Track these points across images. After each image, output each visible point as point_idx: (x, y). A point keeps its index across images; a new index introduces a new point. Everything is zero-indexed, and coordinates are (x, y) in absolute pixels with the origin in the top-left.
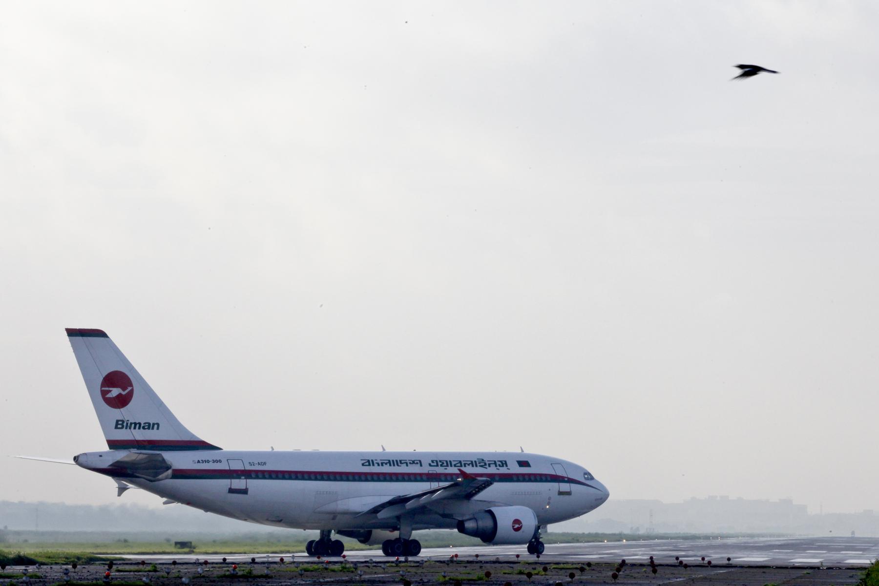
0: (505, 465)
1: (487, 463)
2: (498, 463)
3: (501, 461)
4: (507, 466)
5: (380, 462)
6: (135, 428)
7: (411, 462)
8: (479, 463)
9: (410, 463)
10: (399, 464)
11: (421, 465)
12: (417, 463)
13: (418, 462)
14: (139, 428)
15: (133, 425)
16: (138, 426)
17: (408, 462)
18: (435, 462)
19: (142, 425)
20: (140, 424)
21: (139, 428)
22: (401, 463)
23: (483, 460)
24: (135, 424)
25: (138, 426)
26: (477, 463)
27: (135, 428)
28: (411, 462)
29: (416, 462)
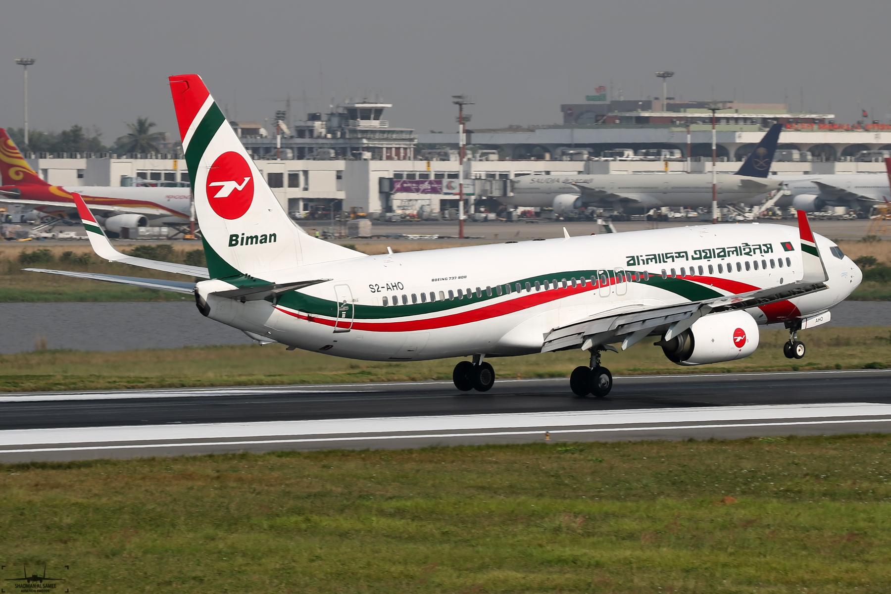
0: (770, 250)
1: (752, 248)
2: (763, 248)
4: (772, 252)
5: (645, 258)
7: (677, 255)
9: (676, 257)
10: (666, 260)
11: (687, 259)
12: (683, 256)
15: (250, 240)
16: (254, 239)
17: (674, 255)
18: (698, 252)
19: (259, 239)
20: (256, 237)
22: (667, 258)
24: (252, 238)
25: (254, 239)
26: (742, 248)
27: (252, 243)
29: (681, 254)
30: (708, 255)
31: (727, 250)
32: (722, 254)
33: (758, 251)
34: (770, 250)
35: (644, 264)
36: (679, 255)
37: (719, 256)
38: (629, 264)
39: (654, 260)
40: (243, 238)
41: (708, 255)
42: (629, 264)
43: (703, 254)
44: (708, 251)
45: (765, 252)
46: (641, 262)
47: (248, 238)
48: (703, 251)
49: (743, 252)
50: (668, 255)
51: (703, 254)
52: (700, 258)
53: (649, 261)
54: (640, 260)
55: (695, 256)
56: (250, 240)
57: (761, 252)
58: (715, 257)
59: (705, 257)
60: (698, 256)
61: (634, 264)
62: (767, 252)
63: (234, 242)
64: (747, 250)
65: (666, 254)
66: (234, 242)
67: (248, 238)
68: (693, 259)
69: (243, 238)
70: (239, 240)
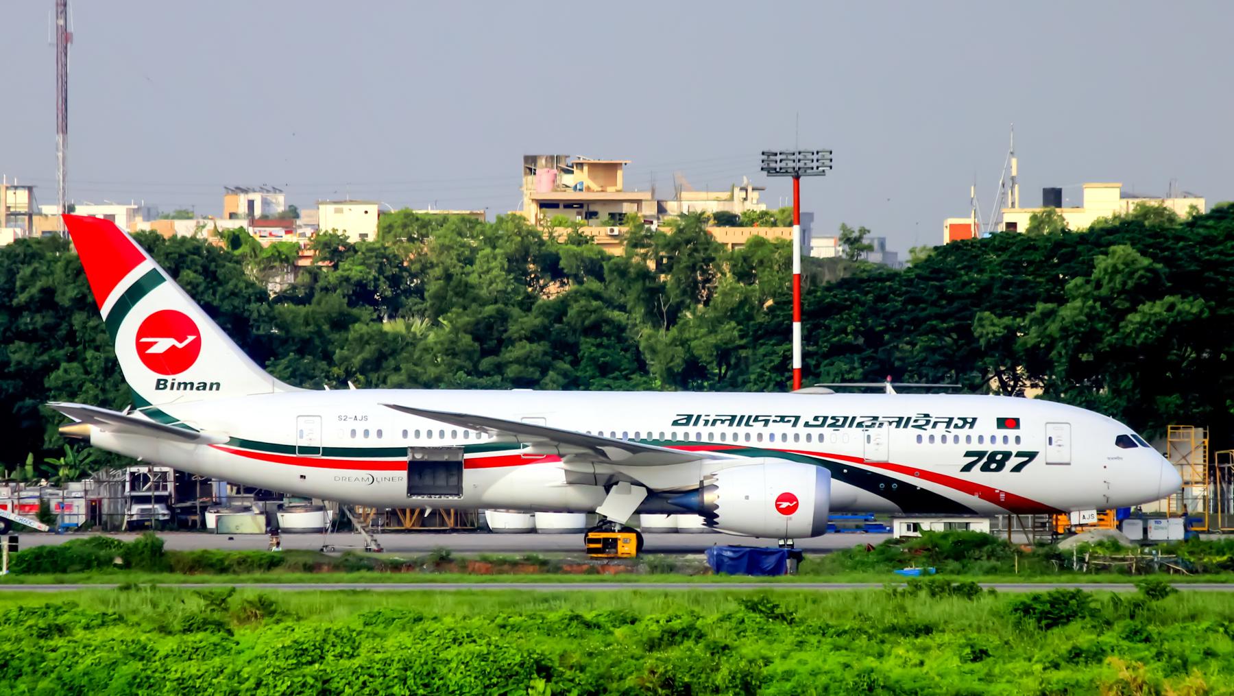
0: (968, 425)
1: (933, 420)
2: (955, 421)
3: (964, 420)
4: (971, 427)
5: (711, 419)
6: (185, 388)
8: (916, 421)
9: (774, 421)
10: (751, 423)
11: (795, 425)
12: (789, 421)
13: (793, 419)
14: (192, 389)
15: (182, 386)
16: (189, 386)
18: (821, 419)
20: (192, 384)
21: (192, 389)
22: (756, 419)
23: (927, 416)
24: (185, 384)
25: (189, 386)
27: (185, 388)
28: (778, 419)
29: (786, 419)
30: (840, 423)
31: (881, 419)
32: (869, 423)
33: (941, 427)
34: (968, 425)
35: (707, 422)
36: (782, 419)
37: (860, 425)
38: (675, 423)
39: (728, 422)
40: (173, 384)
41: (840, 423)
42: (675, 423)
43: (830, 421)
44: (842, 420)
45: (956, 426)
46: (701, 422)
47: (179, 384)
48: (833, 418)
49: (912, 423)
50: (760, 418)
51: (830, 421)
52: (822, 425)
53: (719, 422)
54: (703, 418)
55: (812, 423)
56: (182, 386)
57: (948, 427)
58: (850, 425)
59: (829, 426)
60: (819, 423)
61: (687, 424)
62: (963, 427)
63: (161, 386)
64: (920, 423)
65: (757, 417)
66: (161, 386)
67: (179, 384)
68: (807, 425)
69: (173, 384)
70: (169, 384)
